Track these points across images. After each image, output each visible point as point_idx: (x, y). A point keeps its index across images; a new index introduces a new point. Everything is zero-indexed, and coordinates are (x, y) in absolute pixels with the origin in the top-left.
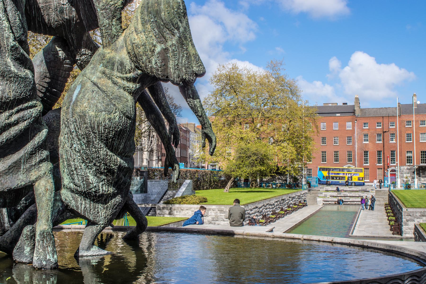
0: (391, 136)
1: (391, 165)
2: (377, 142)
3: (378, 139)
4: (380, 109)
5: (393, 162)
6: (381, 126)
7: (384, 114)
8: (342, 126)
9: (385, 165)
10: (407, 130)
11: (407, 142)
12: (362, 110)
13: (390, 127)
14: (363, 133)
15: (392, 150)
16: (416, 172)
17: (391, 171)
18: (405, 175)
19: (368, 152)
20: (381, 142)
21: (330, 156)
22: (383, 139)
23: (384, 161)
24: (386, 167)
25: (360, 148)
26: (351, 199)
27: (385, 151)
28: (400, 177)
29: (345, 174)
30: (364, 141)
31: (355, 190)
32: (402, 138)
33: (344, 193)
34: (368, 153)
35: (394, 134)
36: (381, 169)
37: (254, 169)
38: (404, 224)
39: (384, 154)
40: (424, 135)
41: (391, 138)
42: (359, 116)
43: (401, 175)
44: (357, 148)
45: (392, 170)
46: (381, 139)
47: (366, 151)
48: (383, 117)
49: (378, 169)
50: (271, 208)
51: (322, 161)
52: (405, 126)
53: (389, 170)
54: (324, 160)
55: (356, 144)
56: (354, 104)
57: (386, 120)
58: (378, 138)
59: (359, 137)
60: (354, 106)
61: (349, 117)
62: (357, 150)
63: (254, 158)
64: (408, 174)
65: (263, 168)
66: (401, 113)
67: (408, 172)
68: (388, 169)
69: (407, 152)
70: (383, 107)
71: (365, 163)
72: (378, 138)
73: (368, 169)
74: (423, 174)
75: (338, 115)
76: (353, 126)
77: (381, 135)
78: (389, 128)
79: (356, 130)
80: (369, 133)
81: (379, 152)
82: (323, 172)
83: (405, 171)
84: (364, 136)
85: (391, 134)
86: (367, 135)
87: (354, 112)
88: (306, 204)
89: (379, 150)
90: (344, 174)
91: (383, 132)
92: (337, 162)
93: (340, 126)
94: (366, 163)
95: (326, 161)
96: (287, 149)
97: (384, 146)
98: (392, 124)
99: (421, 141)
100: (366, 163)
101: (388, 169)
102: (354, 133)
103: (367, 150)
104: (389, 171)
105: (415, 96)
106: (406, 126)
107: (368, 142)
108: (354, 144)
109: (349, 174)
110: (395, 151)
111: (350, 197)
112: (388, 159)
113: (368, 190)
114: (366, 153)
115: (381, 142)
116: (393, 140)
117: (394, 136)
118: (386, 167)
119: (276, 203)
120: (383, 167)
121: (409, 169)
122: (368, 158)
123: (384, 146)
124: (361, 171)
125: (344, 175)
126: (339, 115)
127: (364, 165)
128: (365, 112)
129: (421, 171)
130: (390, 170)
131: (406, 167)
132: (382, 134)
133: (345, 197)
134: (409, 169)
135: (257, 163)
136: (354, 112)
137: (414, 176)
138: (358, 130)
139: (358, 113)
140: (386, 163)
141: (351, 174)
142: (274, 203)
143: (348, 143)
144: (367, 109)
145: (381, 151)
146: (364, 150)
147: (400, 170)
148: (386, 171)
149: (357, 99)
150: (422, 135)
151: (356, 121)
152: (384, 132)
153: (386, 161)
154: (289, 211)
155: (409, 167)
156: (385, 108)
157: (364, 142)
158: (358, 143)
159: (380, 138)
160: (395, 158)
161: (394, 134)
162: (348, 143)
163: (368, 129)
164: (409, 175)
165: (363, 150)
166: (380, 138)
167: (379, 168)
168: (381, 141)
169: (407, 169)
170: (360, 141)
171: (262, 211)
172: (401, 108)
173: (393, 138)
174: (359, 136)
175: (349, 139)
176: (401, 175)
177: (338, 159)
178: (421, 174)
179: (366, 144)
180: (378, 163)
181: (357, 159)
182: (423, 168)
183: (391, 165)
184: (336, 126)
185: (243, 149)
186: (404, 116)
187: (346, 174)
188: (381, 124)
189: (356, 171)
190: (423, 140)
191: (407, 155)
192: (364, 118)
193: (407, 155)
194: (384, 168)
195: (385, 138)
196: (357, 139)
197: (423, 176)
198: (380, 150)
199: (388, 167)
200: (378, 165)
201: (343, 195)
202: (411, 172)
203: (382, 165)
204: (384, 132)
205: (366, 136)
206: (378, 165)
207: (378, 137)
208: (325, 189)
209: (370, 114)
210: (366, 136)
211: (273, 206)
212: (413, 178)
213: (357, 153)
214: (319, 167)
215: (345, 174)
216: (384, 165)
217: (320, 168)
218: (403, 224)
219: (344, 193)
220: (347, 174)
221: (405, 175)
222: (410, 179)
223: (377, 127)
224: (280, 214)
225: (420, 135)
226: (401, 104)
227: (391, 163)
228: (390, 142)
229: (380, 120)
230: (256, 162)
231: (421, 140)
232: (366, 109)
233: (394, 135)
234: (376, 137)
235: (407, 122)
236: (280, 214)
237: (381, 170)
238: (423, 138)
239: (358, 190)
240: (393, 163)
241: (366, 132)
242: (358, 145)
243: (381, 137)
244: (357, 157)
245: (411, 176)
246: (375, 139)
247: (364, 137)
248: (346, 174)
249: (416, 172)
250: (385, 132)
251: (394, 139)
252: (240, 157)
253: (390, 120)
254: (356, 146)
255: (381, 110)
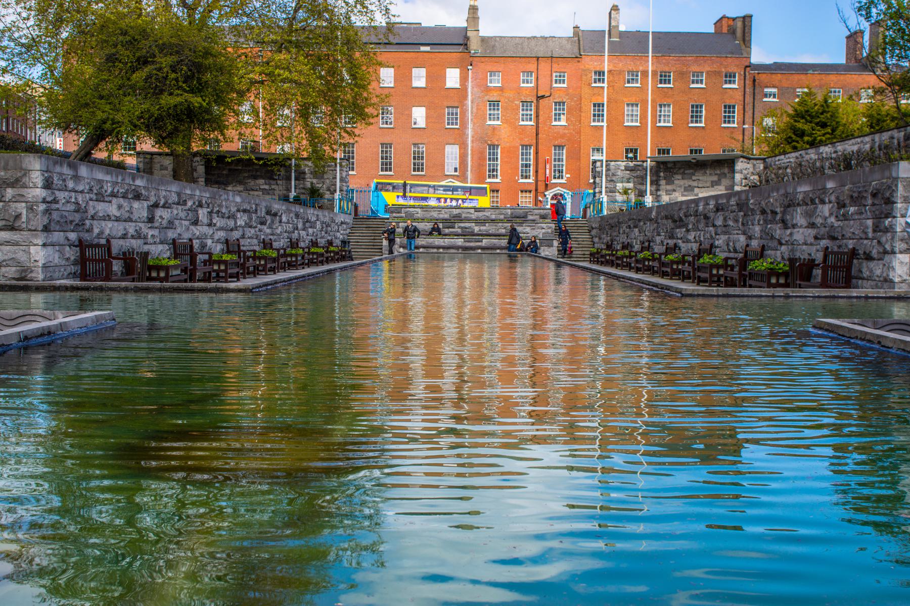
0: (556, 110)
1: (554, 181)
2: (522, 123)
3: (523, 115)
4: (529, 38)
5: (557, 175)
6: (531, 83)
7: (541, 51)
8: (437, 78)
9: (539, 183)
10: (594, 94)
11: (593, 124)
12: (484, 40)
13: (555, 85)
14: (486, 98)
15: (556, 143)
16: (648, 178)
17: (552, 199)
18: (619, 186)
19: (498, 146)
20: (532, 123)
21: (400, 157)
22: (537, 116)
23: (537, 172)
24: (541, 187)
25: (477, 139)
26: (485, 242)
27: (540, 147)
28: (606, 192)
29: (443, 200)
30: (490, 119)
31: (493, 217)
32: (583, 114)
33: (462, 225)
34: (499, 151)
35: (564, 103)
36: (530, 192)
37: (168, 100)
38: (903, 246)
39: (537, 153)
40: (635, 108)
41: (555, 115)
42: (478, 55)
43: (611, 185)
44: (473, 137)
45: (555, 195)
46: (531, 115)
47: (494, 146)
48: (538, 58)
49: (522, 191)
50: (221, 229)
51: (382, 170)
52: (590, 84)
53: (549, 194)
54: (386, 166)
55: (470, 126)
56: (465, 25)
57: (544, 66)
58: (525, 112)
59: (478, 109)
60: (466, 29)
61: (454, 54)
62: (472, 141)
63: (165, 61)
64: (628, 182)
65: (196, 100)
66: (582, 51)
67: (628, 176)
68: (546, 193)
69: (593, 150)
70: (538, 36)
71: (489, 177)
72: (525, 112)
73: (497, 191)
74: (667, 184)
75: (423, 48)
76: (464, 79)
77: (531, 106)
78: (551, 88)
79: (469, 90)
80: (502, 100)
81: (526, 146)
82: (384, 194)
83: (619, 173)
84: (490, 105)
85: (556, 103)
86: (498, 105)
87: (466, 45)
88: (350, 252)
89: (526, 141)
90: (439, 199)
91: (538, 97)
92: (420, 173)
93: (429, 77)
94: (493, 176)
95: (390, 170)
96: (290, 72)
97: (537, 134)
98: (560, 76)
99: (626, 124)
100: (493, 176)
101: (546, 193)
102: (465, 97)
103: (496, 143)
104: (549, 197)
105: (615, 10)
106: (594, 85)
107: (499, 123)
108: (464, 125)
109: (452, 199)
110: (563, 147)
111: (482, 235)
112: (548, 166)
113: (530, 217)
114: (493, 147)
115: (532, 123)
116: (559, 120)
117: (563, 109)
118: (541, 187)
119: (245, 217)
120: (533, 188)
121: (631, 170)
122: (499, 162)
123: (537, 134)
124: (482, 192)
125: (440, 202)
126: (427, 49)
127: (489, 180)
128: (494, 46)
129: (662, 174)
130: (551, 195)
131: (624, 164)
132: (535, 101)
133: (464, 235)
134: (631, 170)
135: (177, 80)
136: (465, 44)
137: (643, 188)
138: (475, 89)
139: (474, 46)
140: (541, 177)
141: (457, 200)
142: (234, 209)
143: (448, 124)
144: (498, 39)
145: (530, 146)
146: (489, 142)
147: (608, 170)
148: (540, 198)
149: (473, 9)
150: (630, 108)
151: (470, 67)
152: (539, 98)
153: (540, 171)
154: (296, 255)
155: (631, 164)
156: (541, 37)
157: (489, 123)
158: (474, 124)
159: (529, 112)
160: (562, 165)
161: (564, 103)
162: (448, 124)
163: (501, 89)
164: (631, 185)
165: (486, 142)
166: (529, 112)
167: (526, 188)
168: (531, 120)
169: (627, 168)
170: (480, 117)
171: (171, 225)
172: (581, 39)
173: (559, 115)
174: (478, 105)
175: (452, 114)
176: (611, 185)
177: (422, 165)
178: (663, 182)
179: (494, 128)
180: (522, 175)
181: (472, 166)
182: (669, 165)
183: (554, 181)
184: (419, 78)
185: (124, 33)
186: (590, 58)
187: (446, 200)
188: (531, 76)
189: (470, 190)
190: (632, 121)
191: (592, 158)
192: (491, 59)
193: (592, 158)
194: (536, 190)
195: (541, 113)
196: (472, 113)
197: (669, 187)
198: (527, 143)
199: (546, 185)
200: (521, 181)
201: (459, 231)
202: (637, 177)
203: (531, 181)
204: (539, 98)
205: (494, 105)
206: (521, 181)
207: (523, 110)
208: (403, 215)
209: (505, 51)
210: (494, 105)
211: (231, 223)
212: (642, 194)
213: (472, 150)
214: (376, 181)
215: (443, 200)
216: (537, 181)
217: (378, 183)
218: (899, 246)
219: (462, 225)
220: (448, 200)
221: (619, 186)
222: (632, 197)
223: (522, 85)
224: (260, 258)
225: (626, 108)
226: (582, 28)
227: (555, 178)
228: (554, 123)
229: (532, 67)
230: (173, 76)
231: (628, 121)
232: (495, 37)
233: (564, 105)
234: (518, 109)
235: (595, 73)
236: (260, 258)
237: (528, 195)
238: (632, 115)
239: (502, 217)
240: (559, 178)
241: (494, 96)
242: (473, 129)
243: (531, 110)
244: (472, 160)
245: (635, 188)
246: (517, 114)
247: (490, 109)
248: (446, 200)
249: (648, 178)
250: (543, 97)
251: (562, 116)
252: (111, 59)
253: (555, 66)
254: (470, 132)
255: (533, 43)
